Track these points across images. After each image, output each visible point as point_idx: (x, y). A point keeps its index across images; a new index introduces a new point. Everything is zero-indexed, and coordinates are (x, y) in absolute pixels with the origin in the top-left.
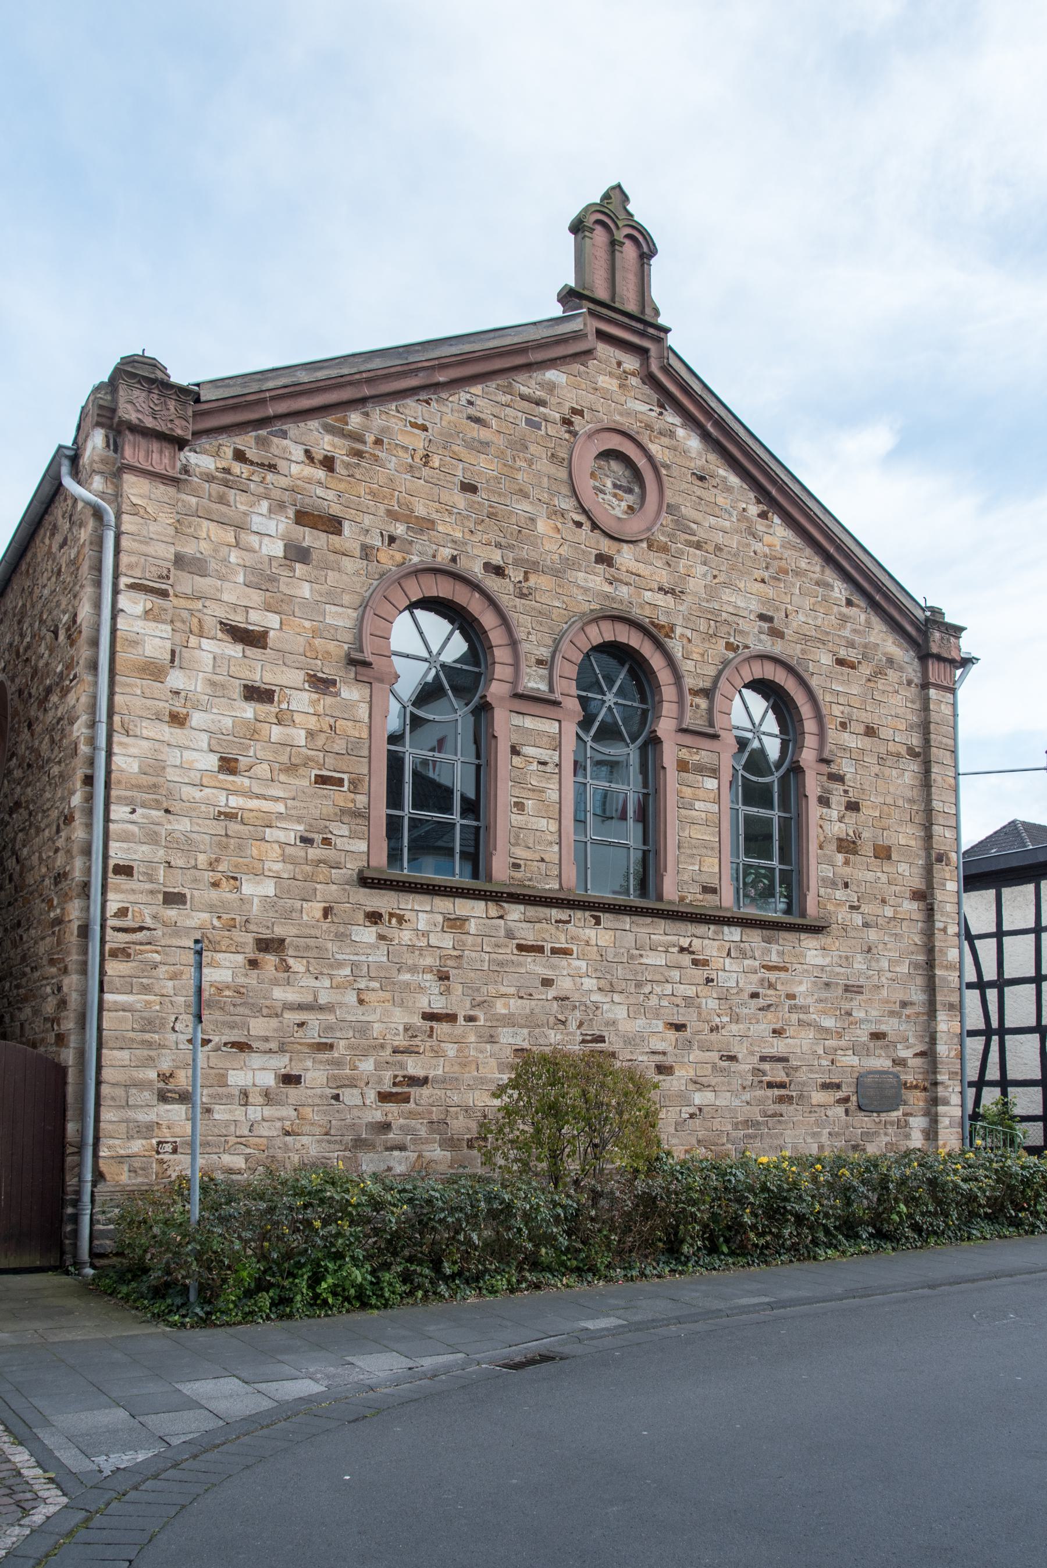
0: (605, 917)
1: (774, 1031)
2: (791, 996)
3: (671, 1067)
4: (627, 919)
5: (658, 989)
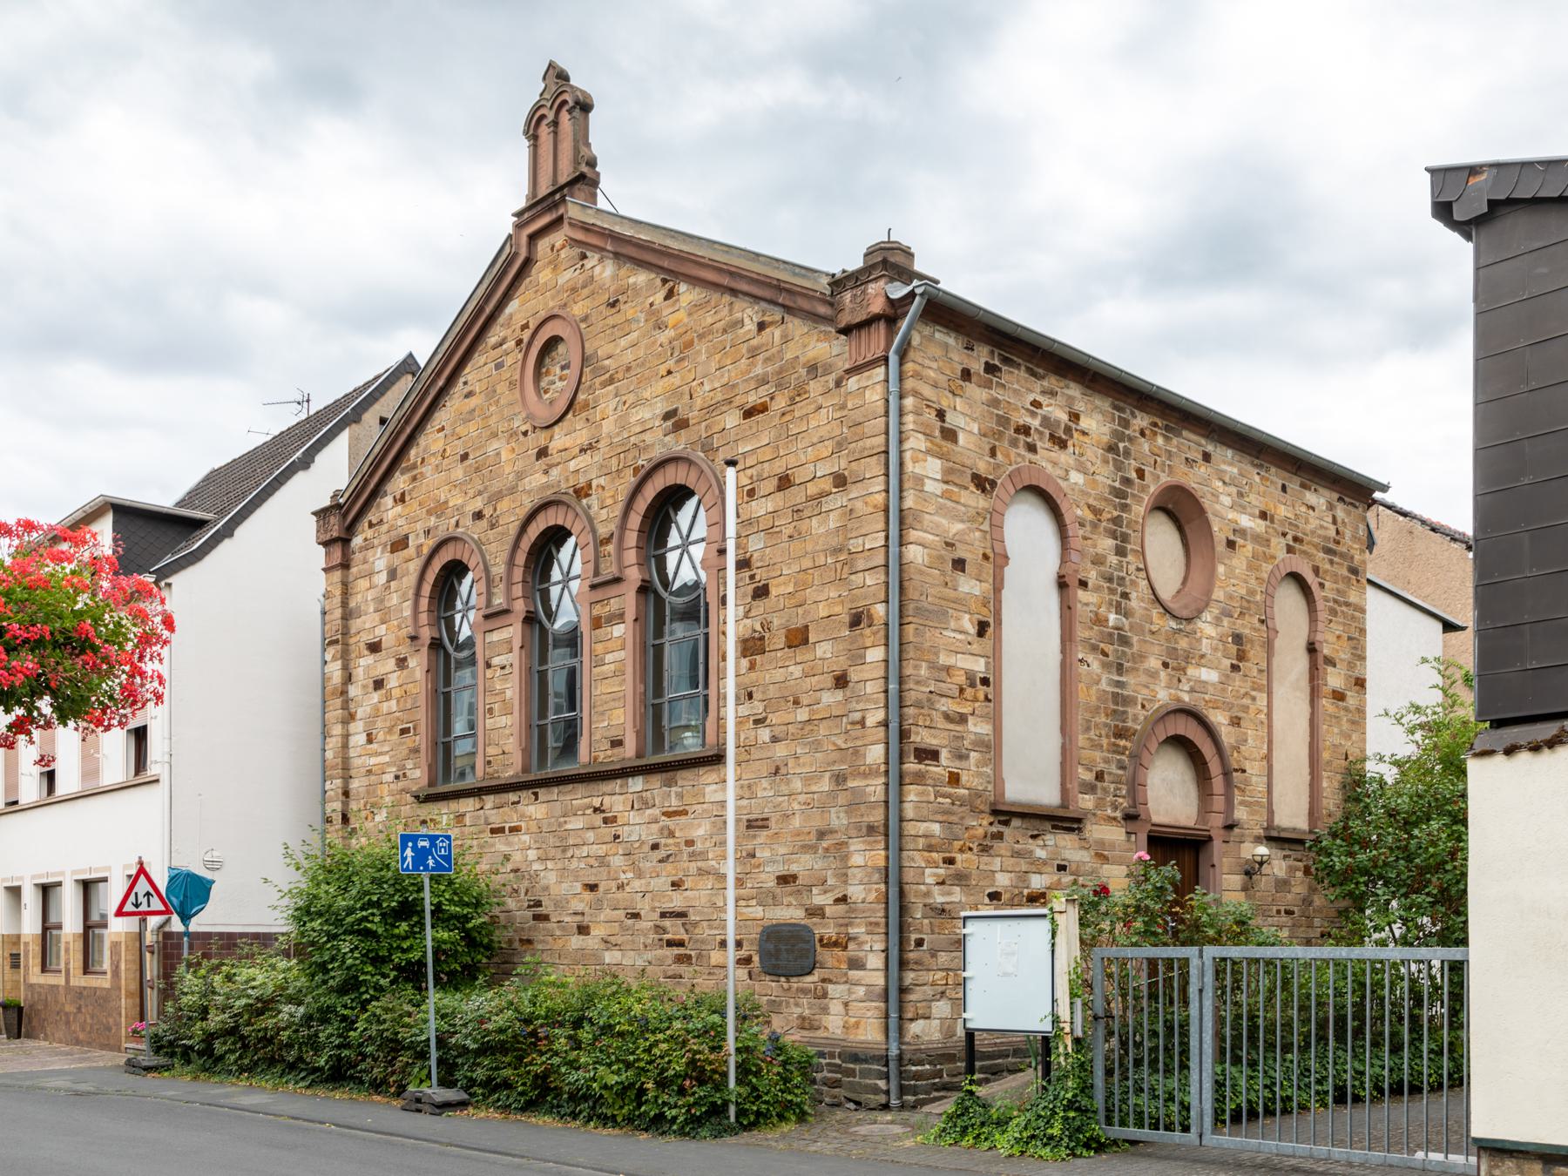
0: (541, 791)
1: (673, 884)
2: (690, 843)
3: (588, 927)
4: (556, 790)
5: (577, 853)
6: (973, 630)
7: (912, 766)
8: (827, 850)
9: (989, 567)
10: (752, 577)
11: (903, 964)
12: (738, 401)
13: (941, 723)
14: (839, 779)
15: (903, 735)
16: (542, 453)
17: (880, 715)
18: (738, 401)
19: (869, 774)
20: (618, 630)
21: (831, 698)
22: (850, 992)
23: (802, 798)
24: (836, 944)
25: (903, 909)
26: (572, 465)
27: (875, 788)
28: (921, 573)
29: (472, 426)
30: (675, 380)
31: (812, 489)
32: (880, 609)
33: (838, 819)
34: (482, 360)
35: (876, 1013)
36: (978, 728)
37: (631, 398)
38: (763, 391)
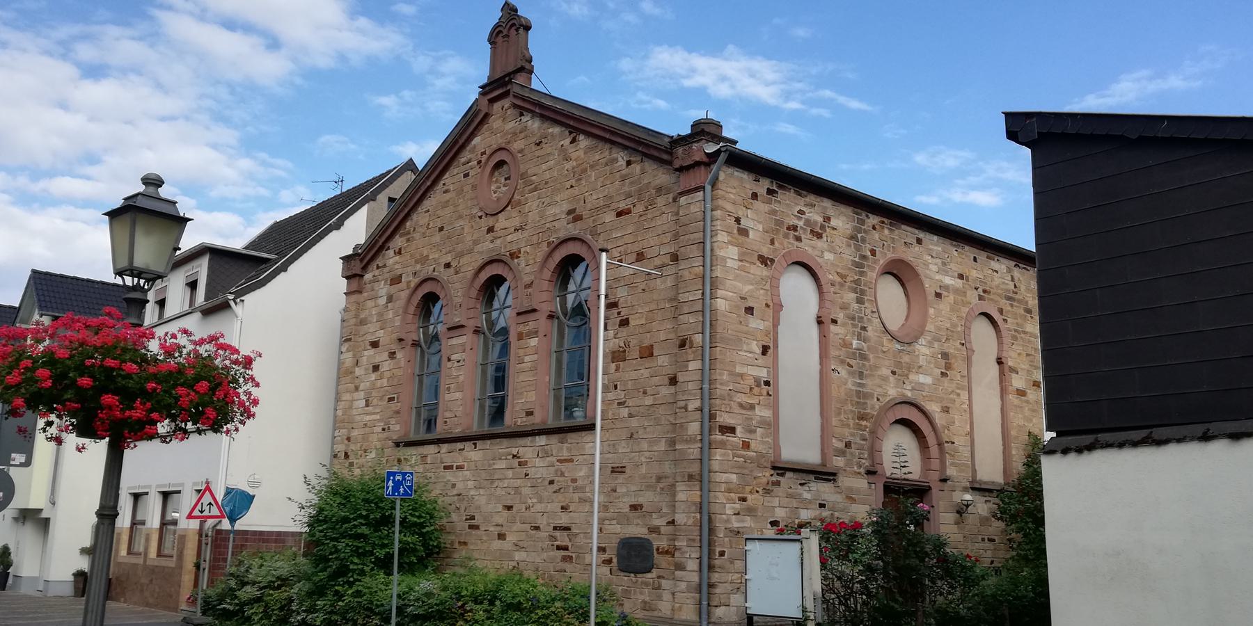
6: (759, 351)
7: (718, 437)
8: (662, 489)
9: (770, 312)
10: (619, 313)
11: (711, 568)
12: (613, 206)
13: (737, 410)
14: (672, 443)
15: (712, 417)
16: (491, 230)
17: (697, 404)
18: (613, 206)
19: (691, 440)
20: (534, 342)
21: (666, 391)
22: (675, 586)
23: (647, 454)
24: (667, 552)
25: (711, 531)
26: (509, 238)
27: (693, 451)
28: (725, 316)
29: (447, 211)
30: (575, 191)
31: (658, 262)
32: (698, 338)
33: (667, 468)
34: (456, 171)
35: (692, 601)
36: (762, 412)
37: (547, 201)
38: (629, 201)
